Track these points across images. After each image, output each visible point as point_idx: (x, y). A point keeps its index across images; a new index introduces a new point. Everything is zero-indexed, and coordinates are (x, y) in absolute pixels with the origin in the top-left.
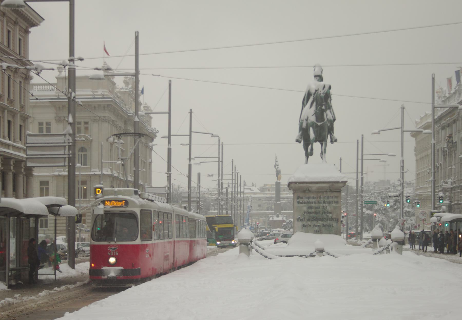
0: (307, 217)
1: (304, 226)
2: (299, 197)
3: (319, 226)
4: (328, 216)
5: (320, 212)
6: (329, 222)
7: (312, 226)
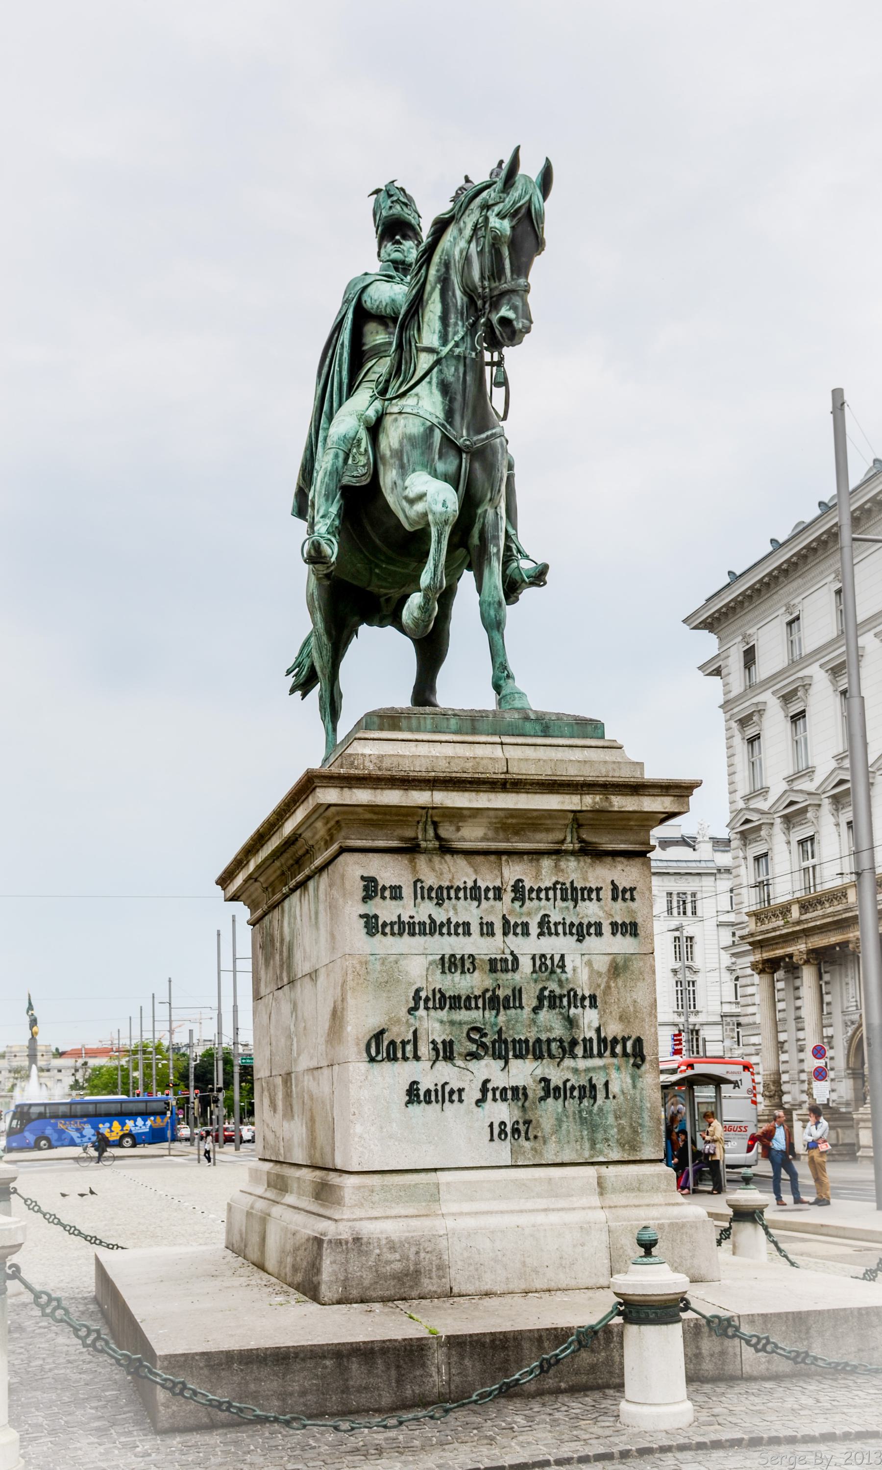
0: (433, 1026)
1: (413, 1094)
2: (371, 889)
3: (517, 1093)
4: (571, 1023)
6: (582, 1064)
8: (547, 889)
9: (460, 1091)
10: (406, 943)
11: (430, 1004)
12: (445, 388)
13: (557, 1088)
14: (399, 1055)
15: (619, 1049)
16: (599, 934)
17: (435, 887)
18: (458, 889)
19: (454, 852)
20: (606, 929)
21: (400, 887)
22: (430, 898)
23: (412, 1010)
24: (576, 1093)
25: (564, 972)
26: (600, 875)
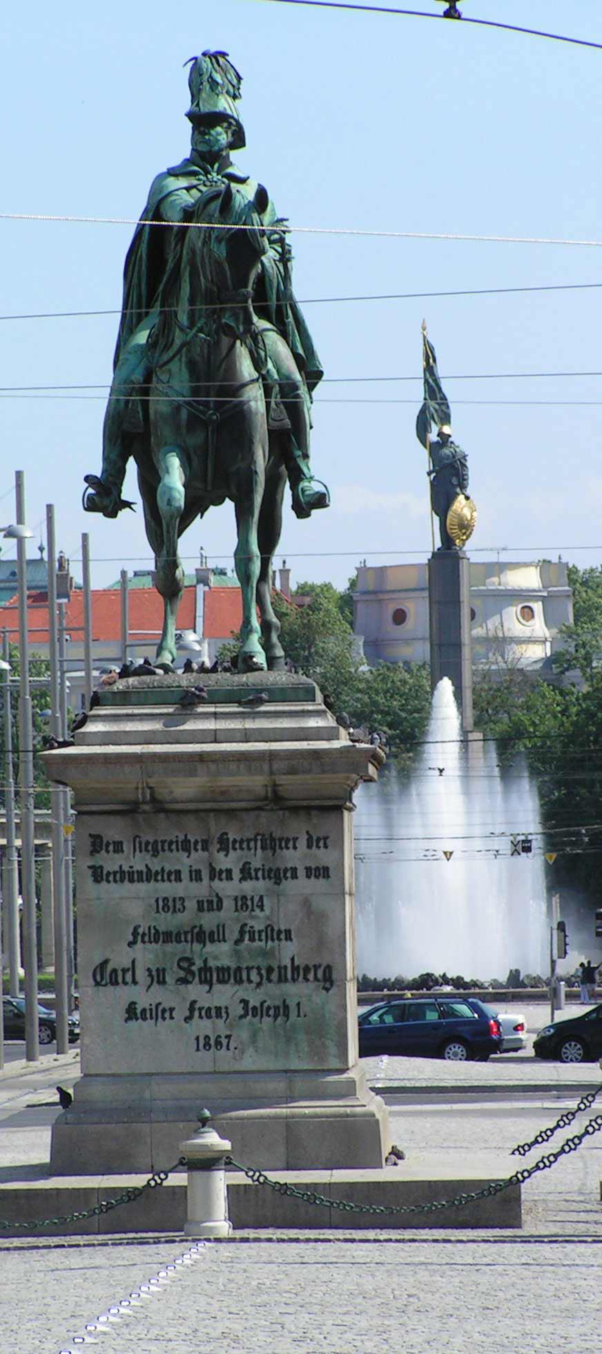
0: (146, 956)
1: (131, 1012)
2: (97, 844)
5: (222, 927)
7: (181, 1012)
8: (249, 841)
9: (172, 1010)
10: (127, 888)
11: (146, 939)
12: (191, 365)
13: (254, 1008)
14: (120, 980)
15: (311, 976)
16: (295, 876)
17: (151, 840)
18: (171, 843)
19: (167, 811)
20: (301, 873)
21: (121, 843)
22: (147, 850)
23: (131, 944)
24: (271, 1012)
25: (262, 910)
26: (298, 828)
